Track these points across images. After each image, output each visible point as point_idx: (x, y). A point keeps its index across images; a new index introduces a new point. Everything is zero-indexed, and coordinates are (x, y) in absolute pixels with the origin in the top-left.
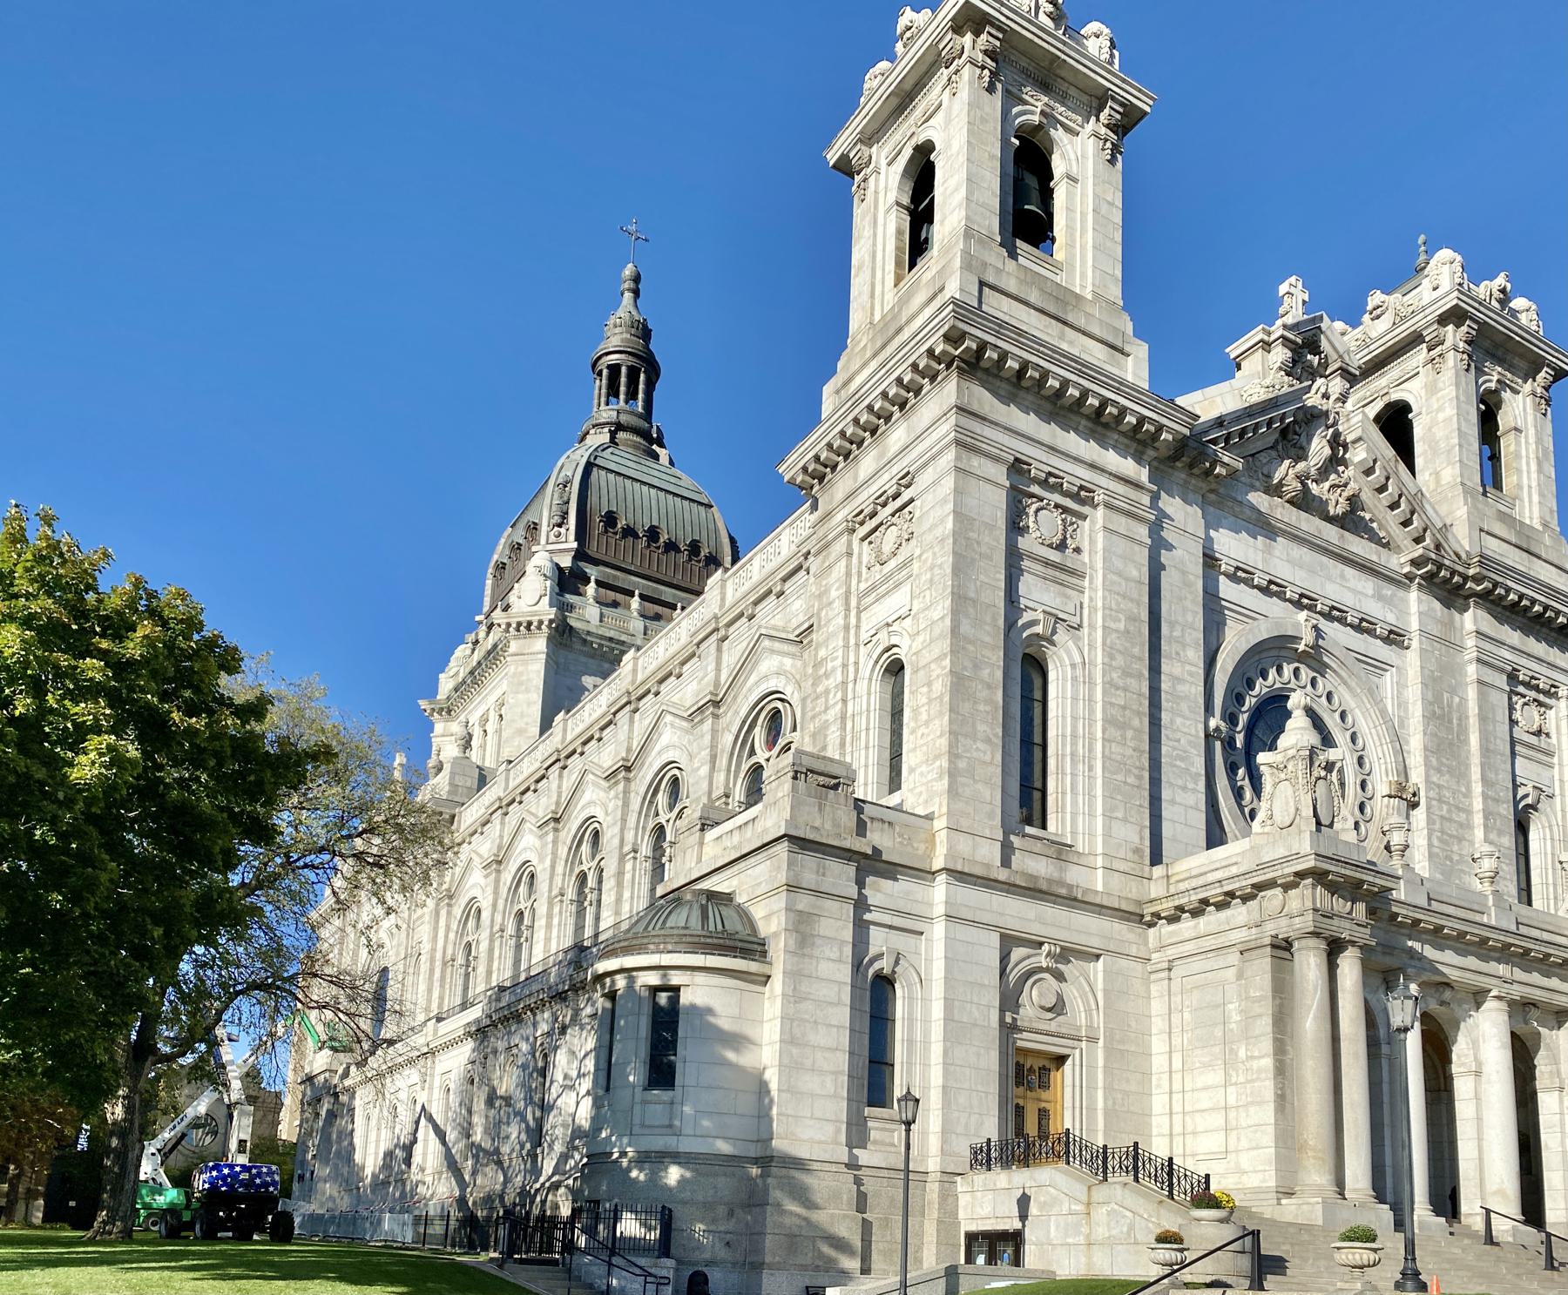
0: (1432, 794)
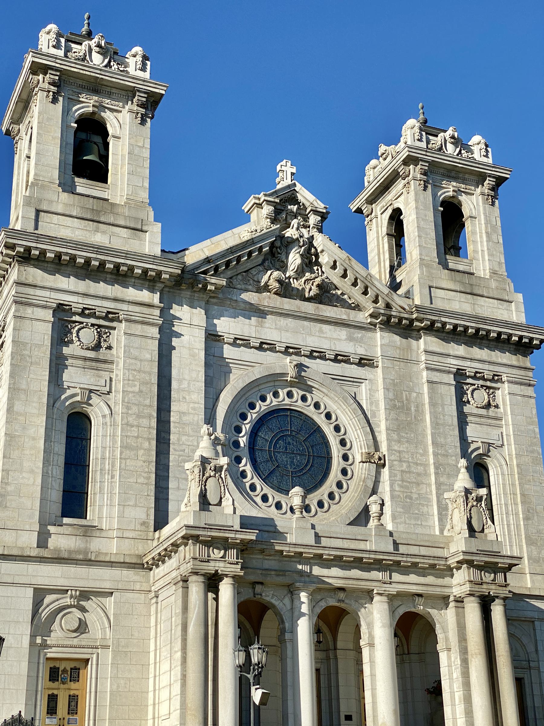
0: (393, 458)
